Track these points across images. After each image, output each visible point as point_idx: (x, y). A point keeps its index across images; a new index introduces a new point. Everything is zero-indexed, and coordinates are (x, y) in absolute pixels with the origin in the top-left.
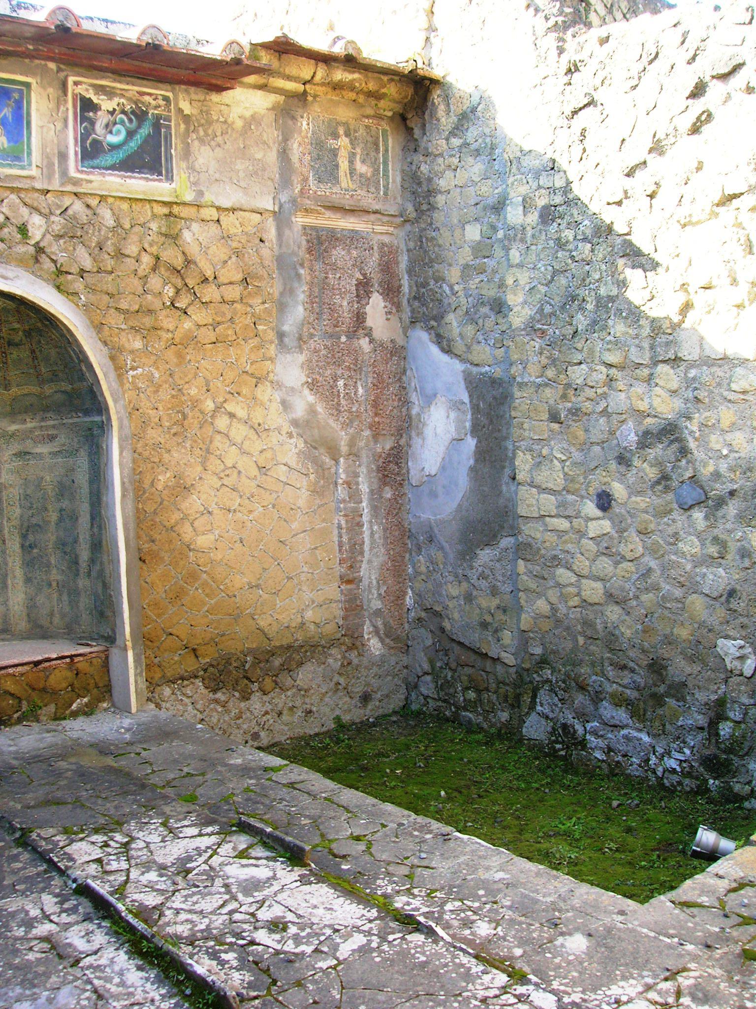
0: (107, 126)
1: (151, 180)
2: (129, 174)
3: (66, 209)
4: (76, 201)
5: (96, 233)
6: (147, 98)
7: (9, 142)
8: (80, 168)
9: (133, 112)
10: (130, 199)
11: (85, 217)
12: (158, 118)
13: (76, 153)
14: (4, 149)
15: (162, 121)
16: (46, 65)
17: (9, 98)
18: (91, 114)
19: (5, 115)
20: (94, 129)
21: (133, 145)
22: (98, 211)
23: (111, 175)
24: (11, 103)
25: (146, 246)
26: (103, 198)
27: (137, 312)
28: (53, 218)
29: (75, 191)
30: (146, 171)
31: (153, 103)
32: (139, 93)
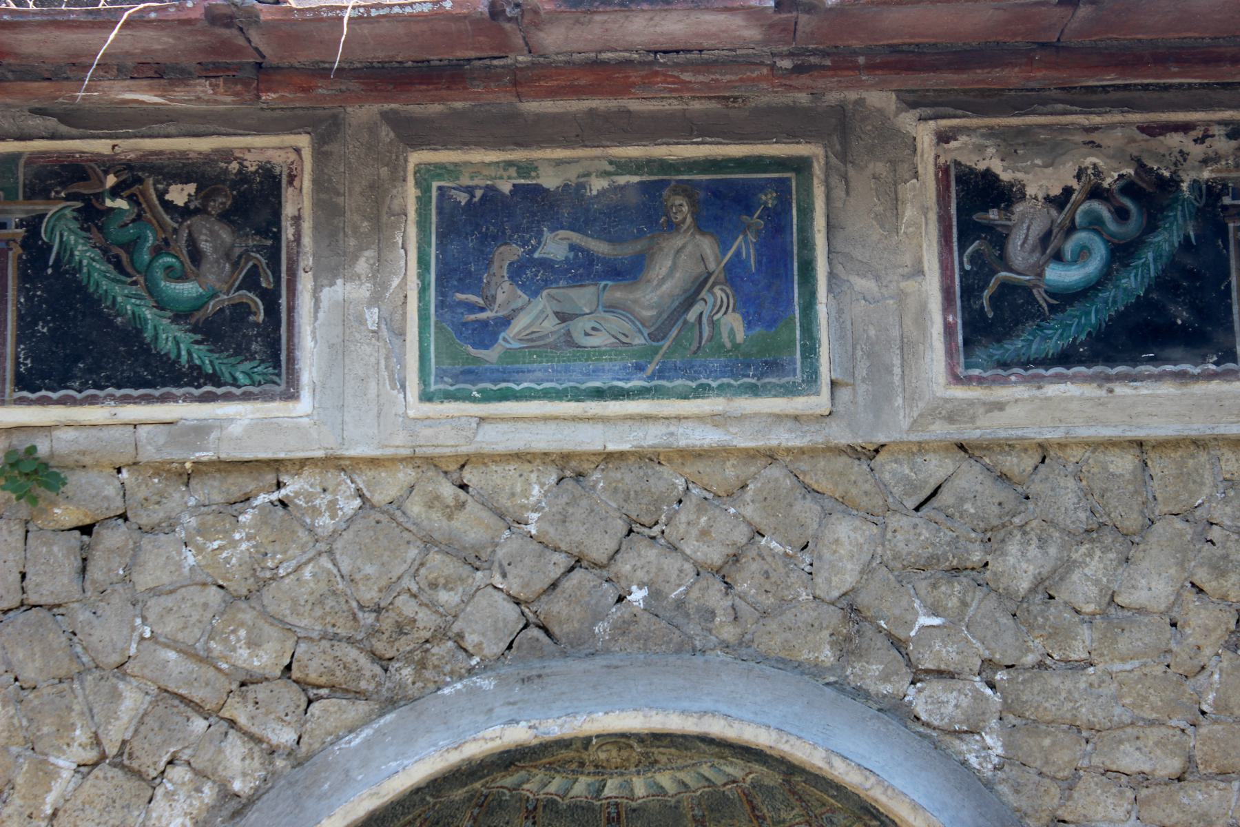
0: (1045, 239)
1: (1196, 378)
2: (1121, 369)
3: (934, 493)
4: (965, 466)
5: (1033, 551)
6: (1175, 140)
7: (749, 325)
8: (960, 371)
9: (1129, 188)
10: (1141, 444)
11: (996, 509)
12: (1211, 193)
13: (949, 330)
14: (736, 346)
15: (1227, 200)
16: (860, 102)
17: (749, 211)
18: (993, 215)
19: (738, 254)
20: (1003, 261)
21: (1132, 283)
22: (1035, 488)
23: (1061, 378)
24: (756, 220)
25: (1202, 577)
26: (1044, 452)
27: (1179, 779)
28: (894, 521)
29: (957, 437)
30: (1178, 352)
31: (1197, 151)
32: (1143, 129)
